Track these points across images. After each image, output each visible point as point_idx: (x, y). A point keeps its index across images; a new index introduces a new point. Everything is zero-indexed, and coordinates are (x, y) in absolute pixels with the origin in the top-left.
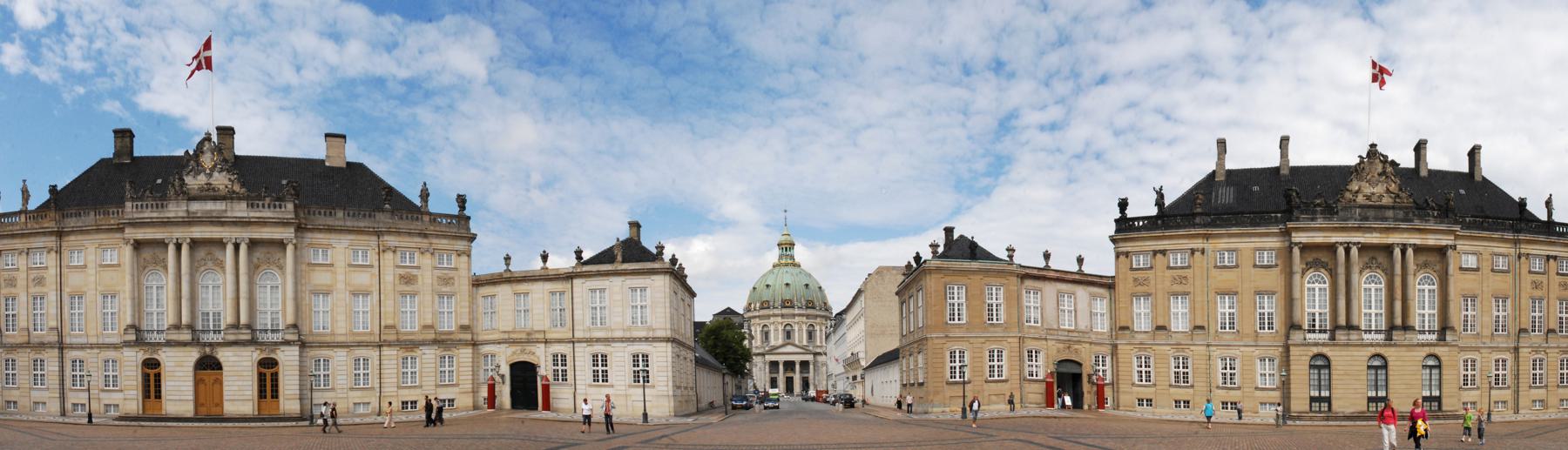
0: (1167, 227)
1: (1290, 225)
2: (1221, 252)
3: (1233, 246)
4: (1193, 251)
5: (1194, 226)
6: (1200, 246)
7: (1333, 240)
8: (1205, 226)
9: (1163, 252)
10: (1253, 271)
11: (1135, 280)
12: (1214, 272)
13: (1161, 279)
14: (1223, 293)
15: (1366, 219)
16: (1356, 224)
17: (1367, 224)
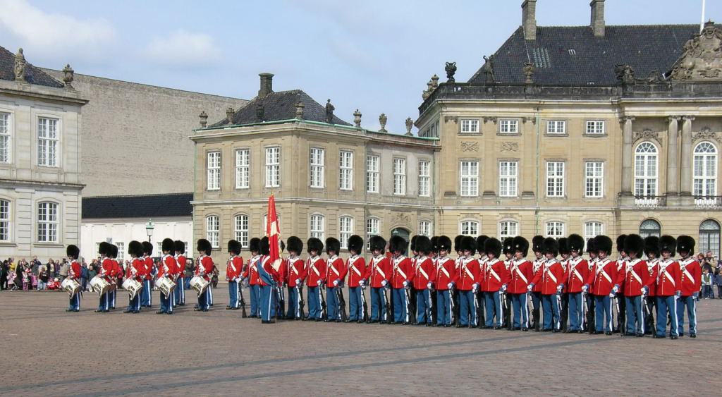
0: (497, 95)
1: (625, 100)
2: (552, 121)
3: (562, 116)
4: (524, 120)
5: (526, 96)
6: (532, 115)
7: (666, 114)
8: (535, 96)
9: (494, 120)
10: (583, 139)
11: (464, 145)
12: (544, 140)
13: (488, 143)
14: (551, 160)
15: (702, 94)
16: (692, 100)
17: (702, 99)
